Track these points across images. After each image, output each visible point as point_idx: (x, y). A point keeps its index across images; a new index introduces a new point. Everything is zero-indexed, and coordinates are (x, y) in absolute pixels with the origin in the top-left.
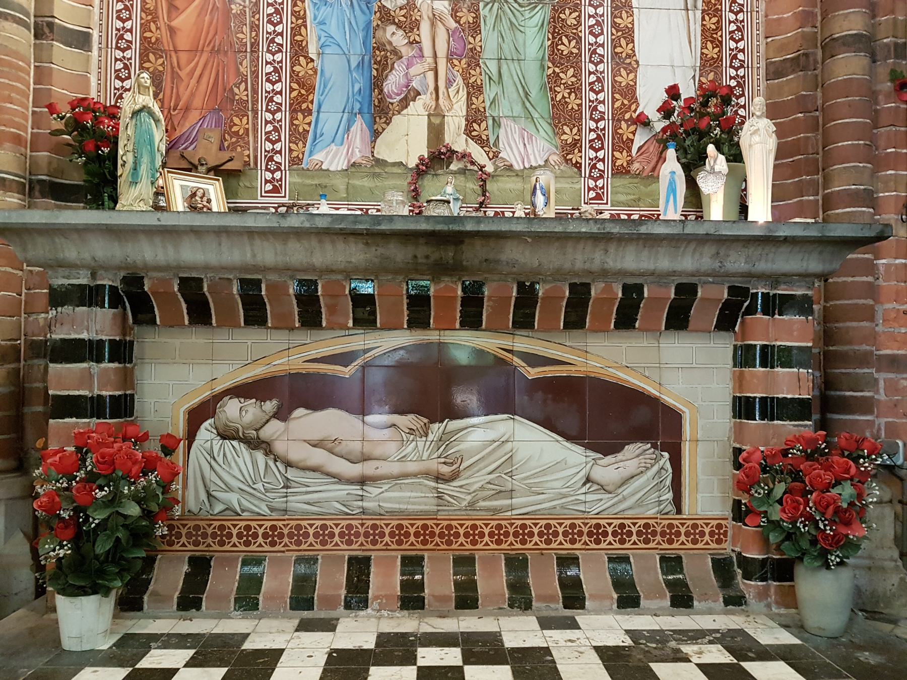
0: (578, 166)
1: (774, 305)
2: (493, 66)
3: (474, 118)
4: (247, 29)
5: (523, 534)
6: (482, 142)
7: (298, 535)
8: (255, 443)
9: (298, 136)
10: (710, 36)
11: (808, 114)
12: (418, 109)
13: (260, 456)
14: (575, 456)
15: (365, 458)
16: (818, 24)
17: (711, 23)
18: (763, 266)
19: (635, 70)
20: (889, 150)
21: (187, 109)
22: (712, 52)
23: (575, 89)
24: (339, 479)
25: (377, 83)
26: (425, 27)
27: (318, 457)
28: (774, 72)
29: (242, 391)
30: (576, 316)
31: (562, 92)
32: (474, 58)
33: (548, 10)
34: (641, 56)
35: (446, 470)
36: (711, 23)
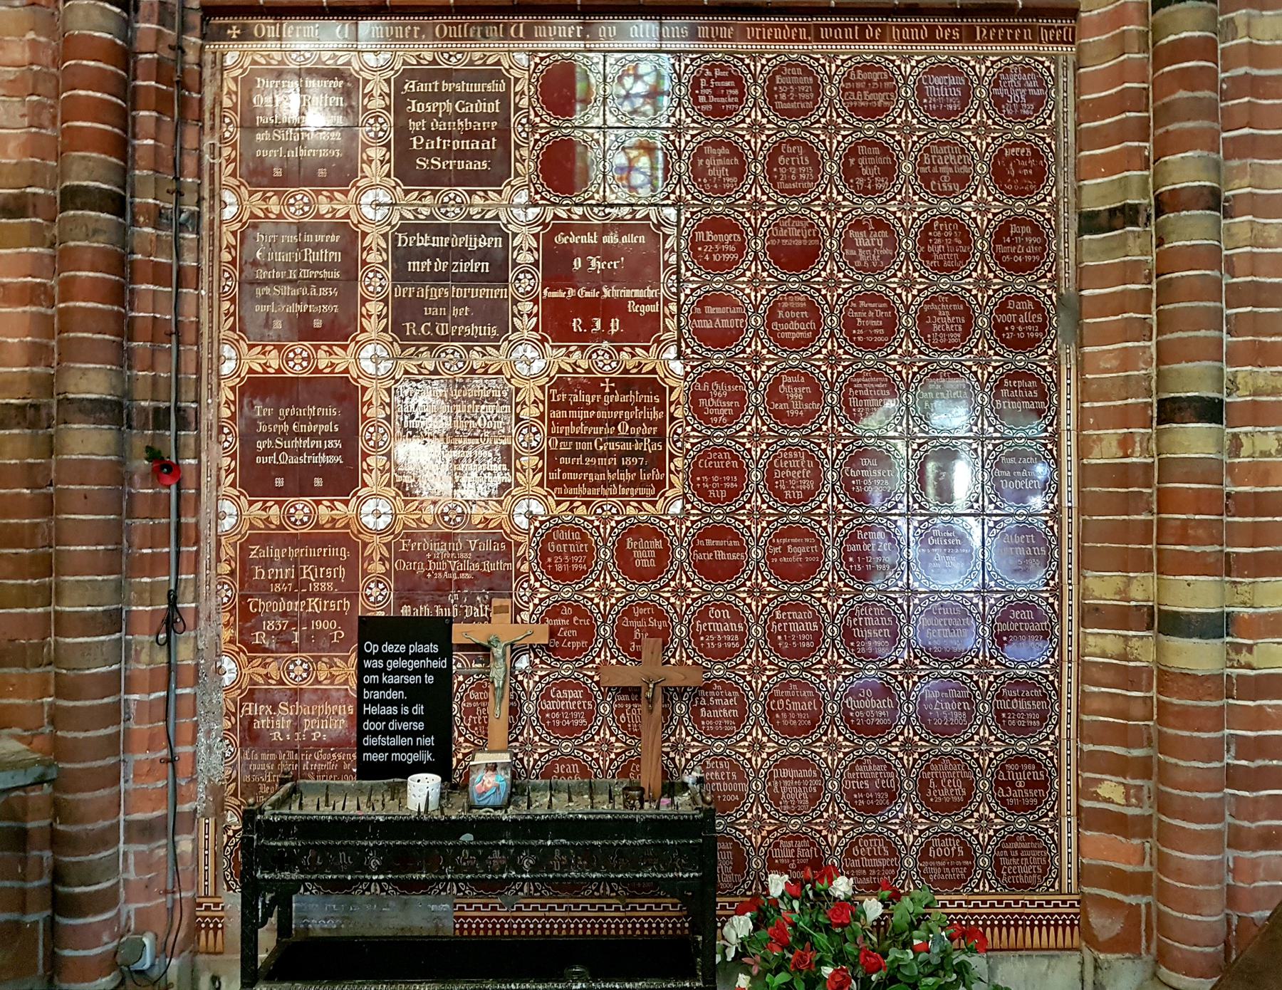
11: (38, 491)
16: (54, 364)
20: (145, 551)
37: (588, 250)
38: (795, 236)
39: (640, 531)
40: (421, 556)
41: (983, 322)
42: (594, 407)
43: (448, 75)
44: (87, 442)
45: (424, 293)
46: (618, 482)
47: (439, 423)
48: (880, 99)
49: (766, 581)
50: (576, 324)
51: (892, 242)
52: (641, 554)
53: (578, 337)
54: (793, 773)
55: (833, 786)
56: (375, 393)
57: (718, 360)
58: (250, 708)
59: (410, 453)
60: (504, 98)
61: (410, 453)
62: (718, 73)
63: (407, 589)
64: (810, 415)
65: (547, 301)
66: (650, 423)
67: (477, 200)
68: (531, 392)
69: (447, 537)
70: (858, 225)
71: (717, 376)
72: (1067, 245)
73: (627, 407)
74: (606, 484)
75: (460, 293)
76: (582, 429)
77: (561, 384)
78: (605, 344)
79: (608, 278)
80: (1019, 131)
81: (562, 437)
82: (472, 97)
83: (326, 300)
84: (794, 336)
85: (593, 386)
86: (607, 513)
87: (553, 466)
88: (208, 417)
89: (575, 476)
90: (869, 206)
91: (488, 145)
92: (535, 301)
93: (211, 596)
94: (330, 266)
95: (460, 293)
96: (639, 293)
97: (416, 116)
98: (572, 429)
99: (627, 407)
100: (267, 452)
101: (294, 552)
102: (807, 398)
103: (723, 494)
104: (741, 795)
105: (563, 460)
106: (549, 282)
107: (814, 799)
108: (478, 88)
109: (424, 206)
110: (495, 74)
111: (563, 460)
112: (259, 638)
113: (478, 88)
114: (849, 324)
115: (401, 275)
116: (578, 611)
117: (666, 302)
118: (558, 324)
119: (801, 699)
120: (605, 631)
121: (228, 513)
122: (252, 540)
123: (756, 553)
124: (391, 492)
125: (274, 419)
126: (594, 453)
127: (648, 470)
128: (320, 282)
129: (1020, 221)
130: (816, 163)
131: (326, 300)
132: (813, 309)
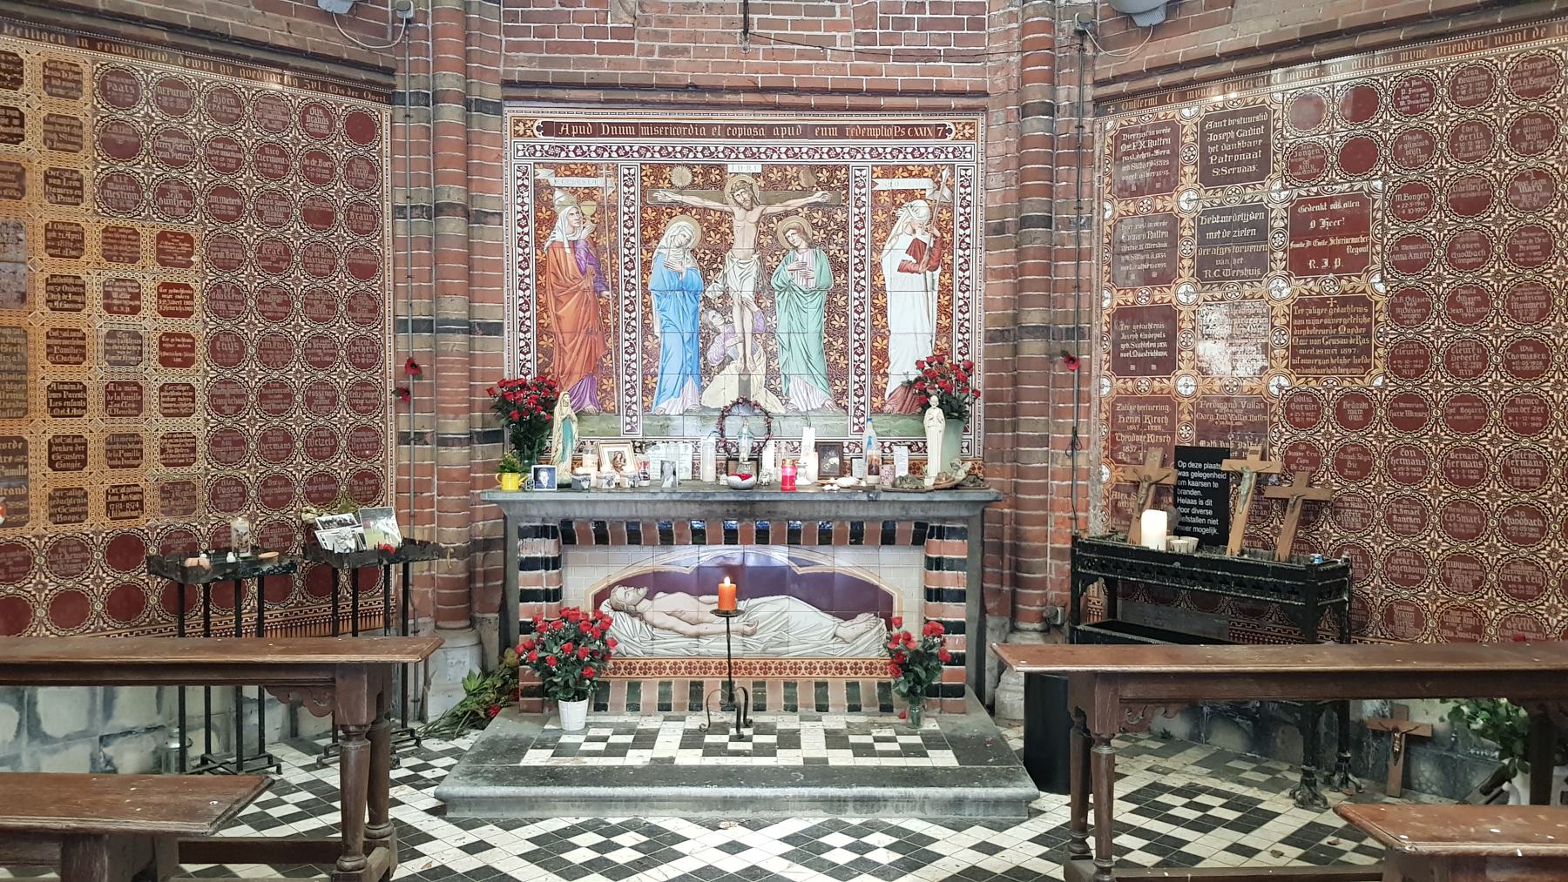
0: (845, 408)
1: (940, 533)
2: (785, 338)
3: (772, 374)
4: (610, 316)
5: (795, 668)
7: (660, 668)
8: (633, 614)
9: (648, 391)
10: (944, 310)
12: (732, 369)
13: (636, 621)
14: (827, 621)
15: (700, 622)
17: (944, 300)
18: (931, 513)
19: (887, 338)
21: (570, 373)
22: (945, 322)
23: (844, 353)
24: (684, 635)
25: (703, 353)
26: (736, 310)
27: (672, 622)
28: (991, 337)
30: (825, 538)
32: (771, 333)
33: (825, 295)
34: (892, 327)
35: (748, 629)
38: (1472, 190)
39: (1356, 397)
40: (1212, 411)
42: (1322, 316)
44: (1033, 348)
45: (1215, 252)
46: (1338, 365)
47: (1225, 331)
48: (1543, 82)
50: (1311, 264)
52: (1353, 411)
53: (1314, 272)
54: (1461, 565)
55: (1492, 577)
56: (1185, 314)
57: (1411, 281)
58: (1116, 495)
59: (1207, 349)
60: (1266, 123)
61: (1207, 349)
62: (1414, 83)
63: (1204, 430)
64: (1480, 316)
65: (1292, 250)
66: (1361, 326)
67: (1249, 190)
68: (1280, 308)
69: (1228, 400)
70: (1522, 177)
71: (1408, 292)
73: (1345, 315)
74: (1329, 366)
75: (1237, 249)
76: (1314, 331)
77: (1301, 303)
78: (1331, 276)
79: (1334, 232)
81: (1300, 337)
82: (1246, 127)
83: (1159, 261)
84: (1468, 261)
85: (1322, 303)
86: (1331, 385)
87: (1294, 355)
88: (1096, 331)
89: (1309, 361)
90: (1532, 162)
91: (1256, 156)
92: (1285, 251)
93: (1095, 432)
94: (1162, 240)
95: (1237, 249)
96: (1355, 240)
97: (1213, 144)
98: (1308, 331)
99: (1345, 315)
100: (1126, 351)
101: (1140, 408)
102: (1478, 305)
103: (1413, 372)
104: (1422, 576)
105: (1302, 352)
106: (1293, 238)
107: (1477, 584)
108: (1250, 120)
109: (1217, 197)
111: (1302, 352)
112: (1121, 456)
113: (1250, 120)
114: (1512, 250)
115: (1203, 242)
116: (1311, 447)
117: (1374, 244)
118: (1298, 265)
119: (1468, 515)
120: (1328, 461)
121: (1106, 386)
122: (1117, 400)
123: (1437, 413)
124: (1195, 372)
125: (1130, 332)
126: (1321, 346)
127: (1359, 357)
128: (1155, 250)
130: (1489, 137)
131: (1159, 261)
132: (1485, 243)
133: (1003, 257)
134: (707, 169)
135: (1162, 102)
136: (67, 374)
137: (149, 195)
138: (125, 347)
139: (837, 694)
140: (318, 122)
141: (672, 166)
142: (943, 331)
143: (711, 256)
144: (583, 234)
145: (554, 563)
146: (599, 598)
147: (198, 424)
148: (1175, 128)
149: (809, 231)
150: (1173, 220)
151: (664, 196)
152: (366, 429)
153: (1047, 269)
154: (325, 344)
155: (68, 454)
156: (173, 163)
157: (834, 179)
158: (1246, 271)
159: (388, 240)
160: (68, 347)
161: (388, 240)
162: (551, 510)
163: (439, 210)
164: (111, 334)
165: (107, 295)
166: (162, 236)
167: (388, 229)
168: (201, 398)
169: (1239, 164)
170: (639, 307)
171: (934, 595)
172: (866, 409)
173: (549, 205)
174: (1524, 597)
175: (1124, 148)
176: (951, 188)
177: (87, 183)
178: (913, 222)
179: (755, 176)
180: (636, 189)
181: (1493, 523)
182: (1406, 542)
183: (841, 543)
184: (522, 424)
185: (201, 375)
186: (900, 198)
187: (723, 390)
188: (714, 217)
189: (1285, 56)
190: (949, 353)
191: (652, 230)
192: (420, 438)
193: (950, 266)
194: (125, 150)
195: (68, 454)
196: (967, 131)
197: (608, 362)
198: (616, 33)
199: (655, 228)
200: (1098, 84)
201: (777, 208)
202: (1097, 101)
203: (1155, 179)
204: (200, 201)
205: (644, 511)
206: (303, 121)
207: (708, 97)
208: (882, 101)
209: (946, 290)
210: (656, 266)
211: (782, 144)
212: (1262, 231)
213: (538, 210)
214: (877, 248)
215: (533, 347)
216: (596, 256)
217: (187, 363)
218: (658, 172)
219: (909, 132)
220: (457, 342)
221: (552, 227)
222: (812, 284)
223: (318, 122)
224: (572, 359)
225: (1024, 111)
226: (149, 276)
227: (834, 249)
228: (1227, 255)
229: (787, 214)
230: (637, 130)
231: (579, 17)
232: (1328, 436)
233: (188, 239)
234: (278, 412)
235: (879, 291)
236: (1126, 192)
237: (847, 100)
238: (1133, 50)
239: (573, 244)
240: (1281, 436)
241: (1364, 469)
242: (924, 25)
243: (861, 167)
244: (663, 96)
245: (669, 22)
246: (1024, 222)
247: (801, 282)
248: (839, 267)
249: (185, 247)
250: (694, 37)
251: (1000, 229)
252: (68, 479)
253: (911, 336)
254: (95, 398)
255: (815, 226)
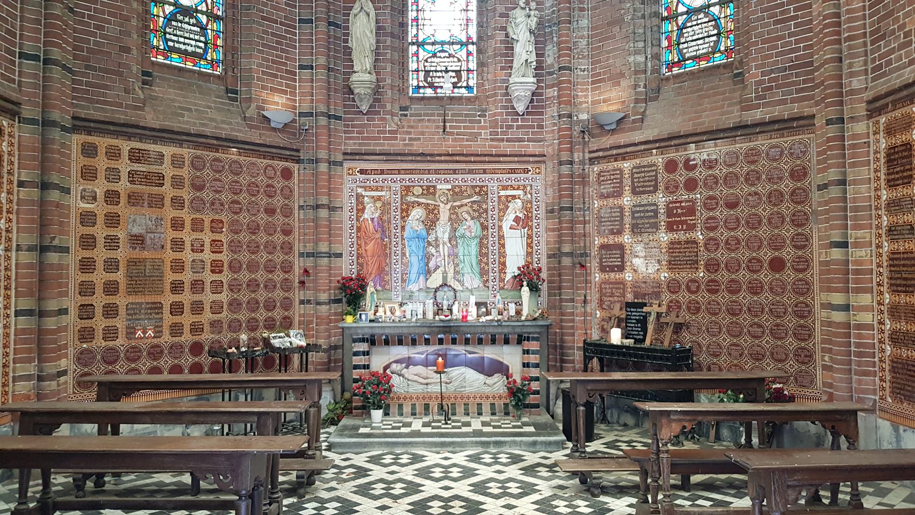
2: (462, 258)
3: (456, 272)
5: (468, 398)
6: (459, 281)
8: (400, 375)
10: (529, 245)
12: (439, 271)
14: (482, 377)
15: (427, 378)
17: (529, 241)
22: (530, 250)
23: (487, 264)
24: (421, 384)
25: (427, 264)
26: (441, 246)
27: (416, 378)
28: (549, 257)
29: (396, 362)
31: (483, 265)
32: (457, 256)
34: (507, 252)
36: (529, 241)
37: (677, 208)
38: (732, 199)
39: (694, 281)
41: (788, 219)
43: (644, 167)
44: (566, 261)
47: (642, 254)
49: (726, 294)
50: (675, 227)
51: (760, 199)
52: (693, 286)
55: (746, 352)
58: (603, 323)
59: (637, 262)
60: (656, 170)
68: (664, 245)
70: (750, 194)
71: (711, 239)
72: (816, 196)
75: (647, 221)
77: (672, 243)
79: (683, 214)
80: (798, 162)
82: (649, 172)
85: (679, 243)
86: (684, 276)
88: (593, 254)
90: (753, 189)
93: (593, 296)
95: (647, 221)
106: (668, 217)
107: (741, 355)
110: (654, 165)
112: (604, 306)
114: (748, 223)
115: (633, 218)
116: (678, 302)
118: (670, 228)
120: (684, 307)
121: (597, 277)
123: (723, 287)
129: (798, 189)
130: (737, 178)
132: (738, 219)
133: (553, 223)
134: (428, 187)
135: (616, 160)
136: (178, 277)
137: (208, 205)
138: (199, 266)
139: (486, 408)
140: (270, 173)
141: (414, 186)
142: (529, 254)
143: (431, 222)
144: (377, 215)
145: (367, 353)
146: (385, 368)
147: (224, 297)
148: (621, 171)
149: (472, 212)
150: (622, 209)
151: (411, 199)
152: (287, 298)
153: (572, 229)
154: (272, 263)
155: (177, 309)
156: (217, 192)
157: (482, 191)
158: (650, 230)
159: (297, 219)
160: (178, 266)
161: (297, 219)
162: (366, 331)
163: (318, 206)
164: (193, 261)
165: (192, 245)
166: (212, 221)
167: (296, 215)
168: (226, 286)
169: (646, 186)
170: (400, 245)
171: (526, 365)
172: (497, 287)
173: (362, 203)
174: (758, 360)
175: (602, 178)
176: (531, 194)
177: (186, 201)
178: (515, 209)
179: (449, 190)
180: (399, 196)
181: (745, 330)
182: (714, 339)
183: (487, 344)
184: (352, 294)
185: (225, 277)
186: (510, 199)
187: (436, 280)
188: (431, 207)
189: (663, 144)
190: (532, 264)
191: (405, 212)
192: (309, 302)
193: (531, 227)
194: (200, 188)
195: (177, 309)
196: (537, 171)
197: (387, 269)
198: (390, 132)
199: (407, 212)
200: (590, 152)
201: (458, 203)
202: (590, 159)
203: (614, 192)
204: (226, 206)
205: (405, 331)
206: (265, 172)
207: (429, 158)
208: (501, 159)
209: (530, 237)
210: (407, 228)
211: (460, 177)
212: (656, 212)
213: (357, 205)
214: (500, 220)
215: (355, 263)
216: (382, 225)
217: (221, 272)
218: (408, 189)
219: (513, 171)
220: (325, 261)
221: (363, 213)
222: (473, 234)
223: (270, 173)
224: (371, 268)
225: (561, 163)
226: (207, 237)
227: (482, 220)
228: (643, 223)
229: (462, 206)
230: (399, 172)
231: (374, 126)
232: (684, 297)
233: (222, 222)
234: (254, 292)
235: (501, 237)
236: (602, 196)
237: (487, 159)
238: (604, 139)
239: (372, 219)
240: (666, 297)
241: (698, 310)
242: (518, 127)
243: (493, 186)
244: (410, 158)
245: (412, 127)
246: (562, 209)
247: (468, 234)
248: (484, 228)
249: (220, 225)
250: (423, 133)
251: (552, 211)
252: (177, 319)
253: (515, 256)
254: (187, 286)
255: (474, 210)
